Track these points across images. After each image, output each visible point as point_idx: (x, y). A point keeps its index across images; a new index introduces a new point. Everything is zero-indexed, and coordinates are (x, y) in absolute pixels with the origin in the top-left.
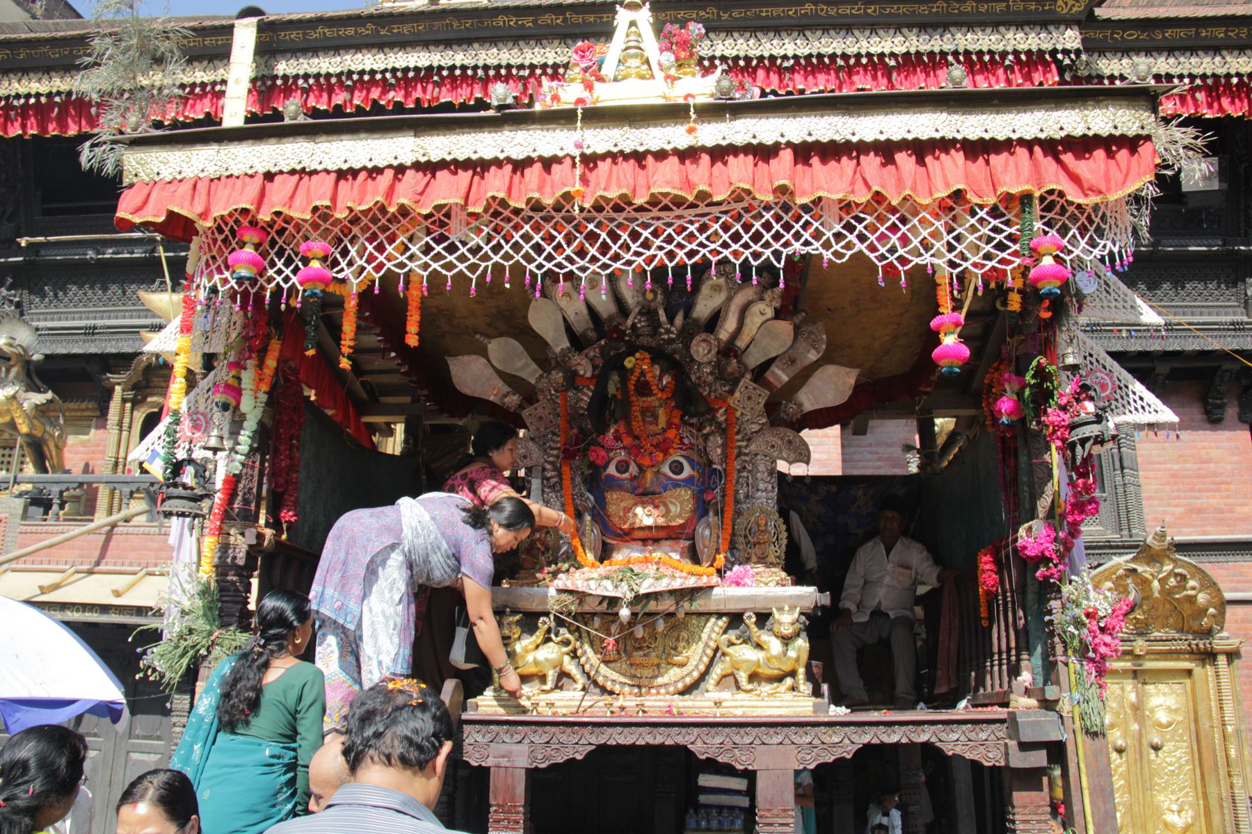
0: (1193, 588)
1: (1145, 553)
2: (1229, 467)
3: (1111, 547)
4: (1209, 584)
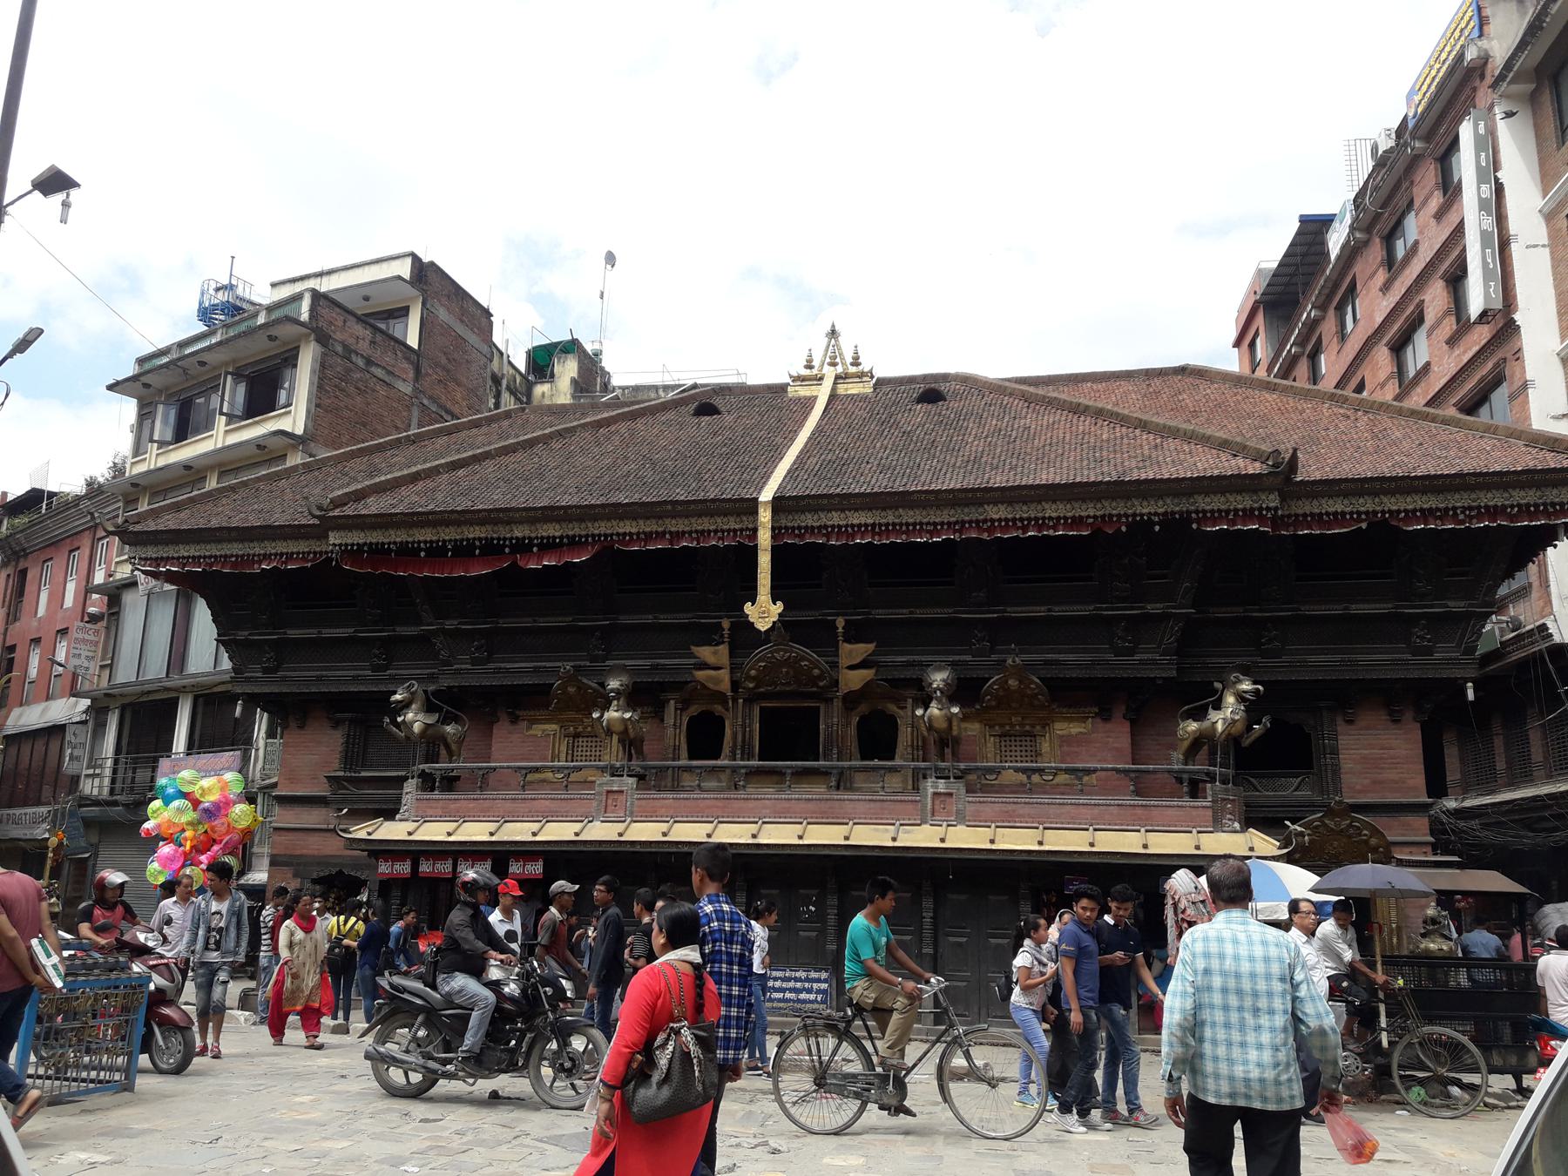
0: (1365, 835)
1: (1330, 812)
2: (1404, 752)
3: (1315, 806)
4: (1375, 832)
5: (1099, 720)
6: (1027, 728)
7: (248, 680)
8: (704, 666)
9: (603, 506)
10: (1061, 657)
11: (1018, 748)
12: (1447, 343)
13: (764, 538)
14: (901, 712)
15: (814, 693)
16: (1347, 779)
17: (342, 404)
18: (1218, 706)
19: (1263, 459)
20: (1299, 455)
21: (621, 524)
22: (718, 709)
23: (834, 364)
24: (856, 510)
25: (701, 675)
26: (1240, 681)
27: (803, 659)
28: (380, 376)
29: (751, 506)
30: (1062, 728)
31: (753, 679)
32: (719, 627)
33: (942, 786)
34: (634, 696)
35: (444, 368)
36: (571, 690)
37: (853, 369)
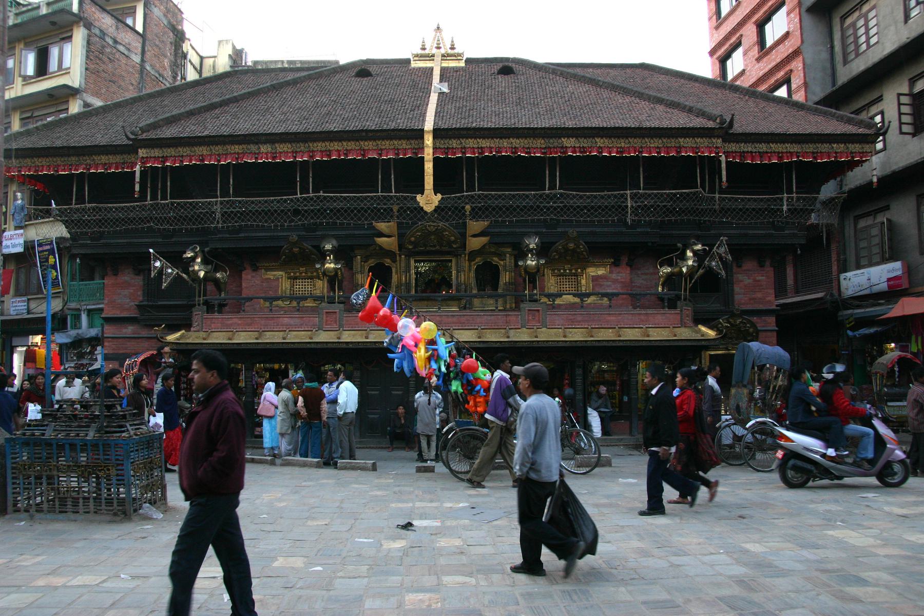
4: (753, 325)
6: (574, 271)
7: (83, 246)
8: (381, 235)
9: (321, 132)
12: (756, 60)
13: (428, 154)
14: (502, 263)
16: (737, 297)
17: (101, 69)
18: (683, 257)
19: (714, 118)
20: (736, 118)
21: (332, 144)
22: (388, 262)
23: (438, 48)
24: (484, 138)
25: (381, 241)
26: (696, 244)
27: (445, 230)
28: (122, 51)
29: (419, 134)
30: (592, 271)
31: (411, 243)
33: (534, 306)
34: (340, 254)
35: (157, 46)
36: (296, 250)
37: (450, 51)
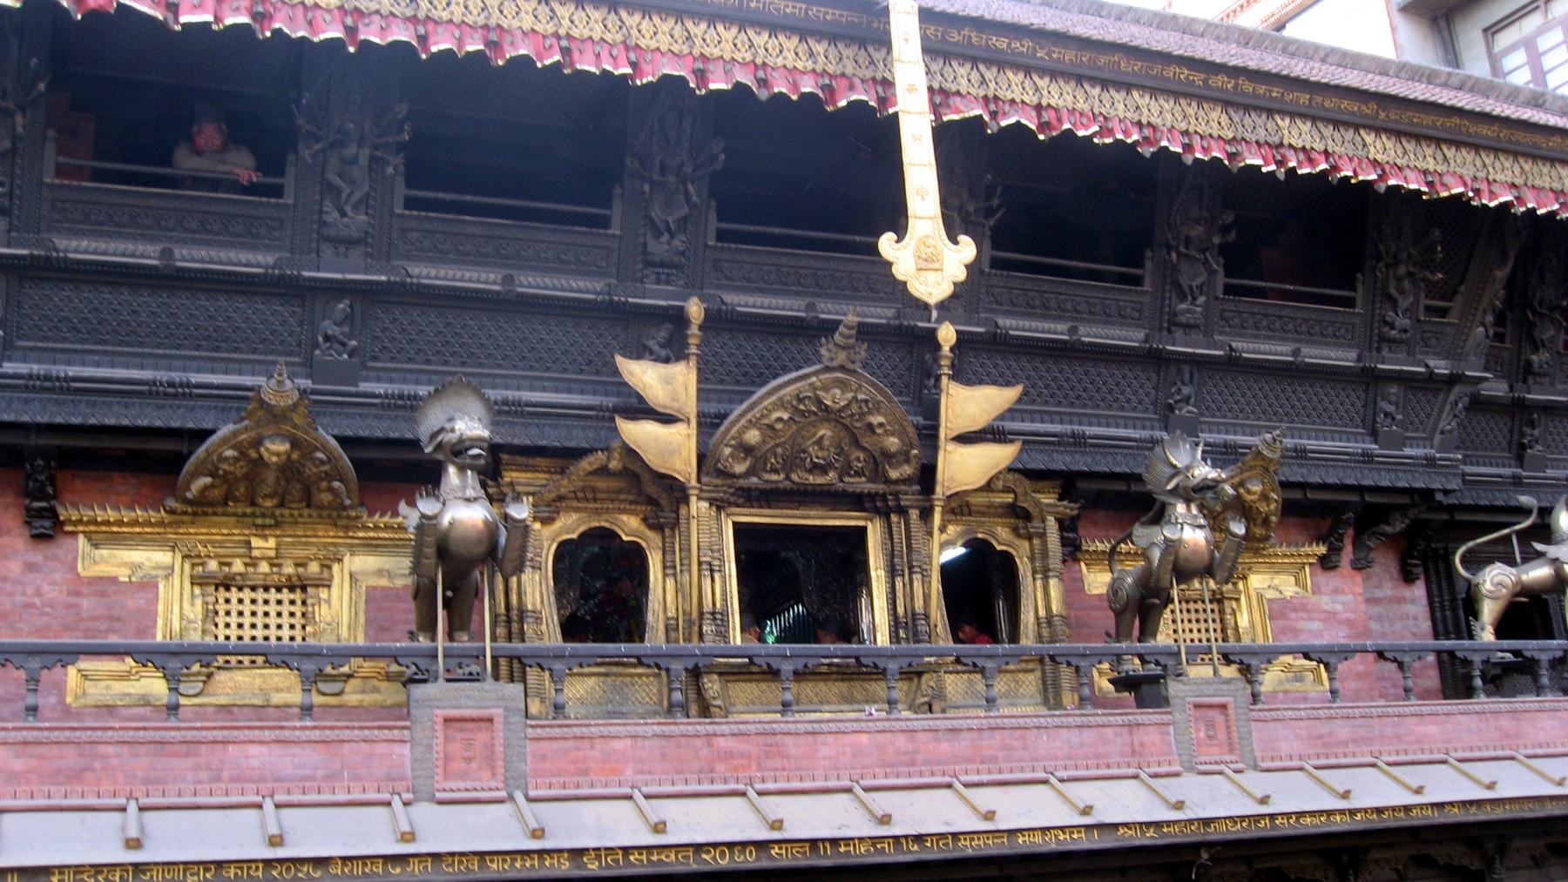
5: (1319, 570)
8: (641, 410)
10: (1311, 444)
11: (1195, 626)
15: (872, 496)
22: (629, 526)
25: (638, 433)
31: (748, 450)
32: (679, 318)
